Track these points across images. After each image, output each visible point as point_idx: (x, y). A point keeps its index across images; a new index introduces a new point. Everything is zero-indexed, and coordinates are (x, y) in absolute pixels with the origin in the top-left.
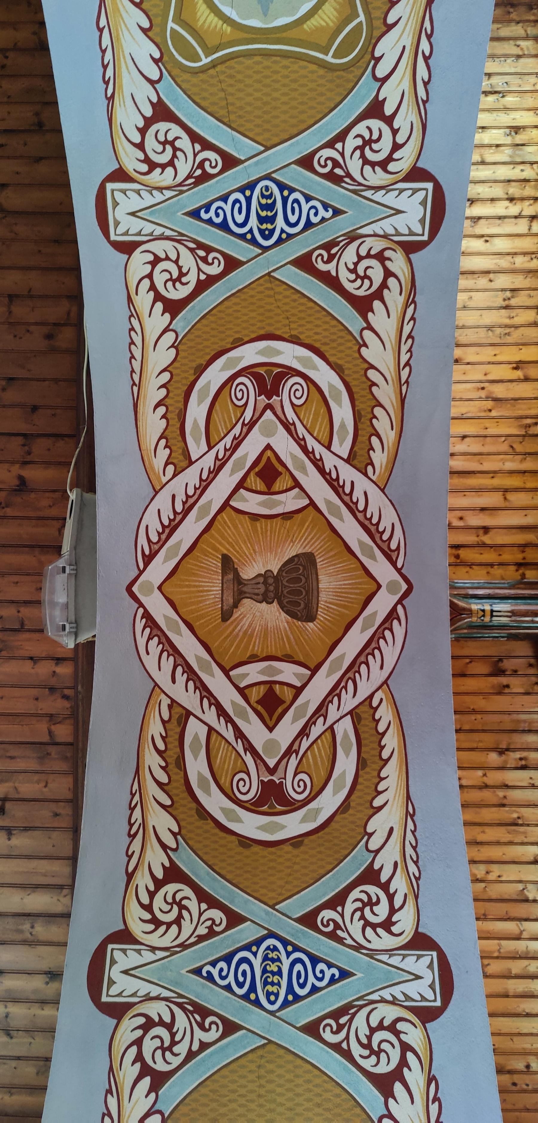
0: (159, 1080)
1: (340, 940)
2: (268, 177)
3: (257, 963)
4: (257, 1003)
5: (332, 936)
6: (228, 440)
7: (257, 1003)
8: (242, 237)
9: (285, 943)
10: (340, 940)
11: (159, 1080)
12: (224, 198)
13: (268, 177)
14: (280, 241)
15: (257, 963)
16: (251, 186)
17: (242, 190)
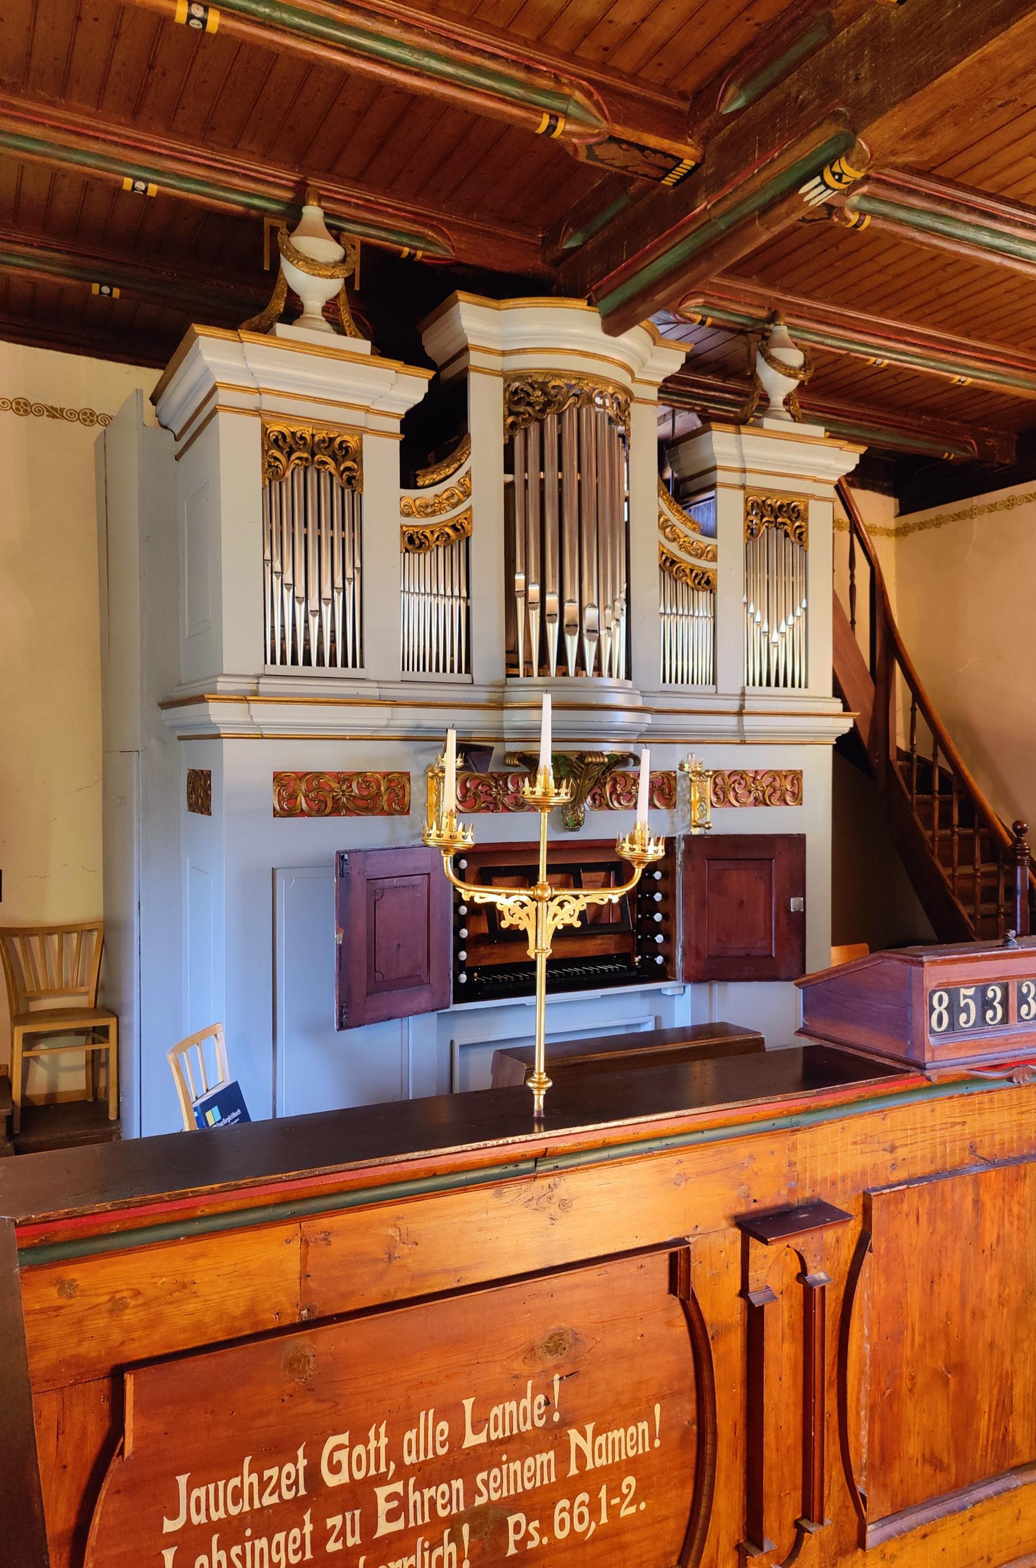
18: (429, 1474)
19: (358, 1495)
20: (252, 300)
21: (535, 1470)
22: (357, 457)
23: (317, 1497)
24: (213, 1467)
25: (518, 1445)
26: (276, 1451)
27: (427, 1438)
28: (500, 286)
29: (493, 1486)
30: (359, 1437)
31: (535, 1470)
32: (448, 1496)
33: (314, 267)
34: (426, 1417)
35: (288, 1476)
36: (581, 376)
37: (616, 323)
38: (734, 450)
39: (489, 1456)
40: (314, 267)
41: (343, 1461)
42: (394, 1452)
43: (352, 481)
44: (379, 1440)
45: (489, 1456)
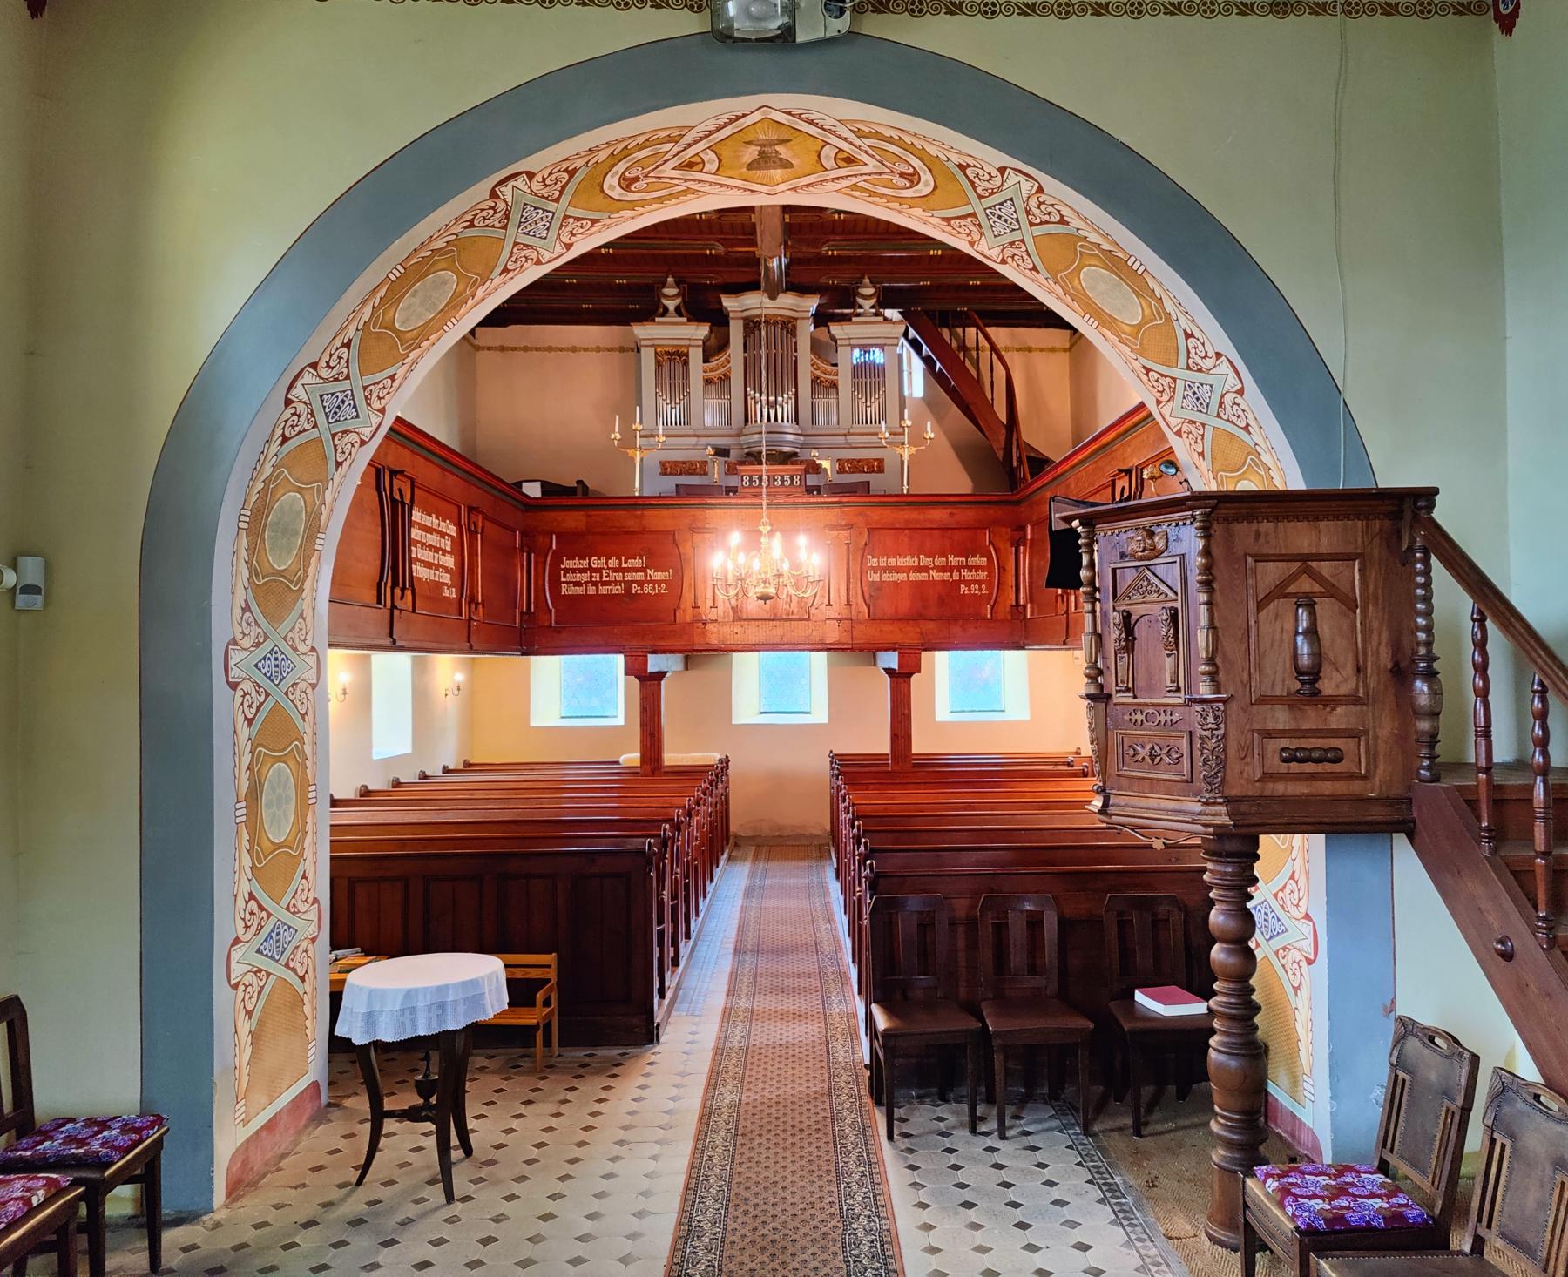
18: (615, 570)
19: (599, 570)
20: (650, 312)
21: (640, 576)
22: (687, 355)
24: (571, 558)
25: (636, 570)
28: (737, 289)
29: (630, 576)
31: (640, 576)
32: (619, 576)
33: (671, 297)
37: (773, 297)
39: (628, 570)
40: (671, 297)
41: (597, 563)
44: (603, 560)
45: (628, 570)
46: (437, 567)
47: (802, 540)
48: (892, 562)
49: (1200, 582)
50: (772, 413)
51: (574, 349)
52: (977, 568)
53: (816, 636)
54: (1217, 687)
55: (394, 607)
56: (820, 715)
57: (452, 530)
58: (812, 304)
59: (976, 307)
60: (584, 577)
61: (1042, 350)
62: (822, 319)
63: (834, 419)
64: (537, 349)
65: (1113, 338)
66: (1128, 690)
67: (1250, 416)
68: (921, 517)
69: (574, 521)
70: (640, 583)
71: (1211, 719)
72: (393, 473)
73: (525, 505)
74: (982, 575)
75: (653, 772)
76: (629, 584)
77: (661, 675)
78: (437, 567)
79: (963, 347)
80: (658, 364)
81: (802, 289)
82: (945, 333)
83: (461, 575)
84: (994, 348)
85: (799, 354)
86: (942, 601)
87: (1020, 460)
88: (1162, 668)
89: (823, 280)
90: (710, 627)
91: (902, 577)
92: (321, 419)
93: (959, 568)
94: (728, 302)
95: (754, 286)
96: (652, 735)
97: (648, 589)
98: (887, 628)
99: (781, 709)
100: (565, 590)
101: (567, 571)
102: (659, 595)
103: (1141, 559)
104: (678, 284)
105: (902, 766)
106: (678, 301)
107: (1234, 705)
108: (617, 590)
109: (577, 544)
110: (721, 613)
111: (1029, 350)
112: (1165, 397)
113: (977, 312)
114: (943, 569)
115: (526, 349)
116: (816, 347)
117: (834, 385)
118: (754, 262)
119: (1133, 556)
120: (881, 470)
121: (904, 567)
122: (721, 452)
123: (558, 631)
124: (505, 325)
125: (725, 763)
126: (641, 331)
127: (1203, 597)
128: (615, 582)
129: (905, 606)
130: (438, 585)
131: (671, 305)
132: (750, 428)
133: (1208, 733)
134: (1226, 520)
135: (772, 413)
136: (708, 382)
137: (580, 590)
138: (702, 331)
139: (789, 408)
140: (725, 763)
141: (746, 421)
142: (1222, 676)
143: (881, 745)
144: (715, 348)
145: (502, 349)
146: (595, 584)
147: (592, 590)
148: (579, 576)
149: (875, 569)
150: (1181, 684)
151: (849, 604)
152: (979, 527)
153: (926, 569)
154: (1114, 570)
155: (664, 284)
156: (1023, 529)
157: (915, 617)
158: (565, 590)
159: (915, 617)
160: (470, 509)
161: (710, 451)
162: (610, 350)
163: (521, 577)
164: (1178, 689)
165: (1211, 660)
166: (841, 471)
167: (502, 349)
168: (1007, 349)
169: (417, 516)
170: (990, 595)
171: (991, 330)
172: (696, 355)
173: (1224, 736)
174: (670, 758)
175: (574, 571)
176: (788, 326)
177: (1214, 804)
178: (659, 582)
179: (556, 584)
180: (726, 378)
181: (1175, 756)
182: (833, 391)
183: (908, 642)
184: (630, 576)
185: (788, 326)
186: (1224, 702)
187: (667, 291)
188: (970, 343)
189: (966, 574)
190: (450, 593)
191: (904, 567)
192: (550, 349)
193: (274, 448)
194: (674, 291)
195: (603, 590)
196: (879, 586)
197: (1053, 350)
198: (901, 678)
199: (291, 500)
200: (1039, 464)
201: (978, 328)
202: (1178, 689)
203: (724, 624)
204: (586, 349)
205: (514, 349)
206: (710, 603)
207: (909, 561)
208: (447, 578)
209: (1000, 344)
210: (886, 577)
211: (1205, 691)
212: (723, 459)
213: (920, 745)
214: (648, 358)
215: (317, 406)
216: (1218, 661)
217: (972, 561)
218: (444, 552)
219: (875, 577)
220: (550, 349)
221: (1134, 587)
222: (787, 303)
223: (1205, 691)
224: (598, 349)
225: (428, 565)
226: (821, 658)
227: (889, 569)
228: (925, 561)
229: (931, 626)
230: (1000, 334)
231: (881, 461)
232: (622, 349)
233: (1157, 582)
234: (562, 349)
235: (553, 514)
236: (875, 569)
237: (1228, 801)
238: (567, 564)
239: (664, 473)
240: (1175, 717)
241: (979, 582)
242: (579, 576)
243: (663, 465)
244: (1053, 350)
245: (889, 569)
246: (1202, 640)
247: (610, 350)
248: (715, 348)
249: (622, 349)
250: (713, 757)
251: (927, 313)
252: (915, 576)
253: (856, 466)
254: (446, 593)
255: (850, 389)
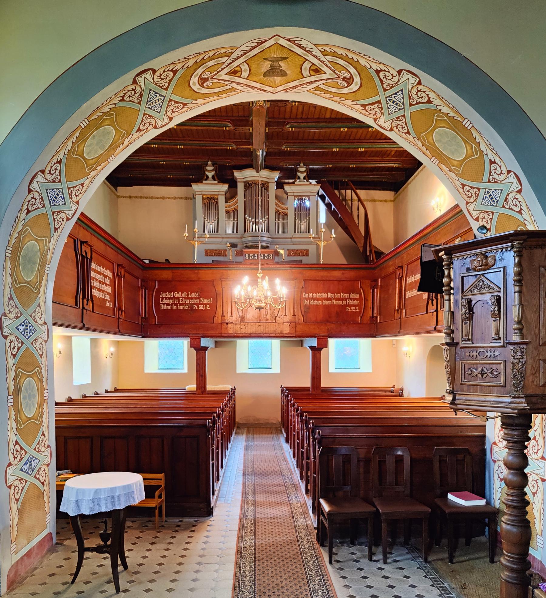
0: (123, 100)
1: (167, 107)
2: (404, 108)
3: (157, 98)
4: (147, 103)
5: (168, 106)
6: (330, 66)
7: (147, 103)
8: (392, 95)
9: (163, 100)
10: (167, 107)
11: (123, 100)
12: (403, 98)
13: (404, 108)
14: (387, 101)
15: (157, 98)
16: (403, 104)
17: (403, 102)
18: (185, 298)
19: (178, 298)
20: (200, 178)
21: (197, 301)
22: (217, 199)
23: (174, 297)
24: (165, 292)
26: (170, 292)
27: (185, 295)
29: (192, 301)
30: (178, 293)
31: (197, 301)
32: (187, 301)
34: (185, 293)
35: (171, 295)
36: (254, 180)
37: (258, 172)
38: (290, 189)
41: (177, 295)
42: (181, 295)
43: (217, 203)
44: (180, 293)
46: (104, 292)
47: (278, 281)
48: (315, 296)
49: (515, 281)
50: (257, 227)
51: (163, 198)
52: (354, 299)
53: (279, 330)
54: (522, 336)
55: (83, 308)
56: (276, 369)
57: (110, 274)
58: (276, 175)
59: (351, 179)
60: (171, 301)
61: (381, 201)
62: (280, 185)
63: (286, 231)
64: (147, 198)
65: (446, 169)
66: (469, 340)
67: (524, 205)
68: (329, 275)
69: (166, 275)
70: (197, 305)
71: (519, 353)
72: (82, 243)
73: (143, 266)
74: (357, 302)
75: (202, 393)
76: (192, 305)
77: (206, 348)
78: (104, 292)
79: (345, 199)
80: (204, 204)
81: (272, 168)
82: (336, 192)
83: (115, 296)
84: (359, 200)
85: (270, 199)
86: (338, 314)
87: (371, 252)
88: (489, 327)
89: (281, 164)
90: (229, 325)
91: (319, 303)
92: (47, 203)
93: (346, 299)
94: (237, 174)
95: (250, 166)
96: (202, 376)
97: (201, 307)
98: (312, 327)
99: (258, 366)
100: (162, 307)
101: (163, 298)
102: (206, 310)
103: (479, 270)
104: (213, 165)
105: (316, 391)
106: (213, 173)
107: (530, 346)
108: (186, 307)
109: (168, 286)
110: (234, 319)
111: (375, 201)
112: (472, 200)
113: (351, 181)
114: (338, 299)
115: (141, 197)
116: (277, 197)
117: (286, 214)
118: (251, 154)
119: (475, 270)
120: (307, 255)
121: (321, 298)
122: (233, 245)
123: (159, 326)
124: (131, 186)
125: (234, 390)
126: (196, 187)
127: (517, 289)
128: (186, 304)
129: (320, 317)
130: (104, 300)
131: (210, 175)
132: (247, 234)
133: (516, 361)
134: (530, 247)
135: (257, 227)
136: (227, 212)
137: (169, 308)
138: (225, 187)
139: (265, 225)
140: (234, 390)
141: (245, 231)
142: (524, 331)
143: (307, 383)
144: (231, 195)
145: (130, 197)
146: (176, 305)
147: (175, 307)
148: (168, 301)
149: (307, 299)
150: (501, 335)
151: (294, 315)
152: (356, 280)
153: (330, 299)
154: (462, 278)
155: (207, 165)
156: (376, 281)
157: (326, 322)
158: (162, 307)
159: (326, 322)
160: (118, 265)
161: (228, 244)
162: (180, 198)
163: (141, 300)
164: (499, 338)
165: (519, 322)
166: (289, 255)
167: (130, 197)
168: (365, 200)
169: (94, 265)
170: (360, 312)
171: (358, 191)
172: (221, 200)
173: (526, 362)
174: (210, 387)
175: (166, 298)
176: (265, 186)
177: (519, 397)
178: (206, 304)
179: (158, 304)
180: (236, 211)
181: (495, 373)
182: (286, 217)
183: (322, 334)
184: (192, 301)
185: (265, 186)
186: (526, 344)
187: (208, 168)
188: (348, 197)
189: (349, 302)
190: (109, 305)
191: (321, 298)
192: (152, 198)
193: (23, 215)
194: (212, 168)
195: (180, 307)
196: (308, 307)
197: (386, 201)
198: (316, 351)
199: (31, 244)
200: (379, 254)
201: (352, 189)
202: (499, 338)
203: (236, 324)
204: (169, 198)
205: (136, 197)
206: (229, 314)
207: (322, 295)
208: (108, 298)
209: (362, 198)
210: (312, 303)
211: (516, 338)
212: (234, 249)
213: (324, 383)
214: (199, 200)
215: (44, 195)
216: (523, 322)
217: (352, 296)
218: (107, 285)
219: (306, 303)
220: (152, 198)
221: (474, 286)
222: (265, 174)
223: (516, 338)
224: (175, 198)
225: (99, 290)
226: (276, 343)
227: (313, 299)
228: (330, 295)
229: (332, 326)
230: (362, 193)
231: (307, 251)
232: (186, 198)
233: (488, 282)
234: (158, 198)
235: (157, 272)
236: (307, 299)
237: (526, 396)
238: (163, 295)
239: (207, 255)
240: (497, 353)
241: (355, 306)
242: (168, 301)
243: (206, 251)
244: (386, 201)
245: (313, 299)
246: (515, 312)
247: (180, 198)
248: (231, 195)
249: (186, 198)
250: (228, 387)
251: (328, 181)
252: (325, 303)
253: (296, 253)
254: (108, 305)
255: (293, 216)
